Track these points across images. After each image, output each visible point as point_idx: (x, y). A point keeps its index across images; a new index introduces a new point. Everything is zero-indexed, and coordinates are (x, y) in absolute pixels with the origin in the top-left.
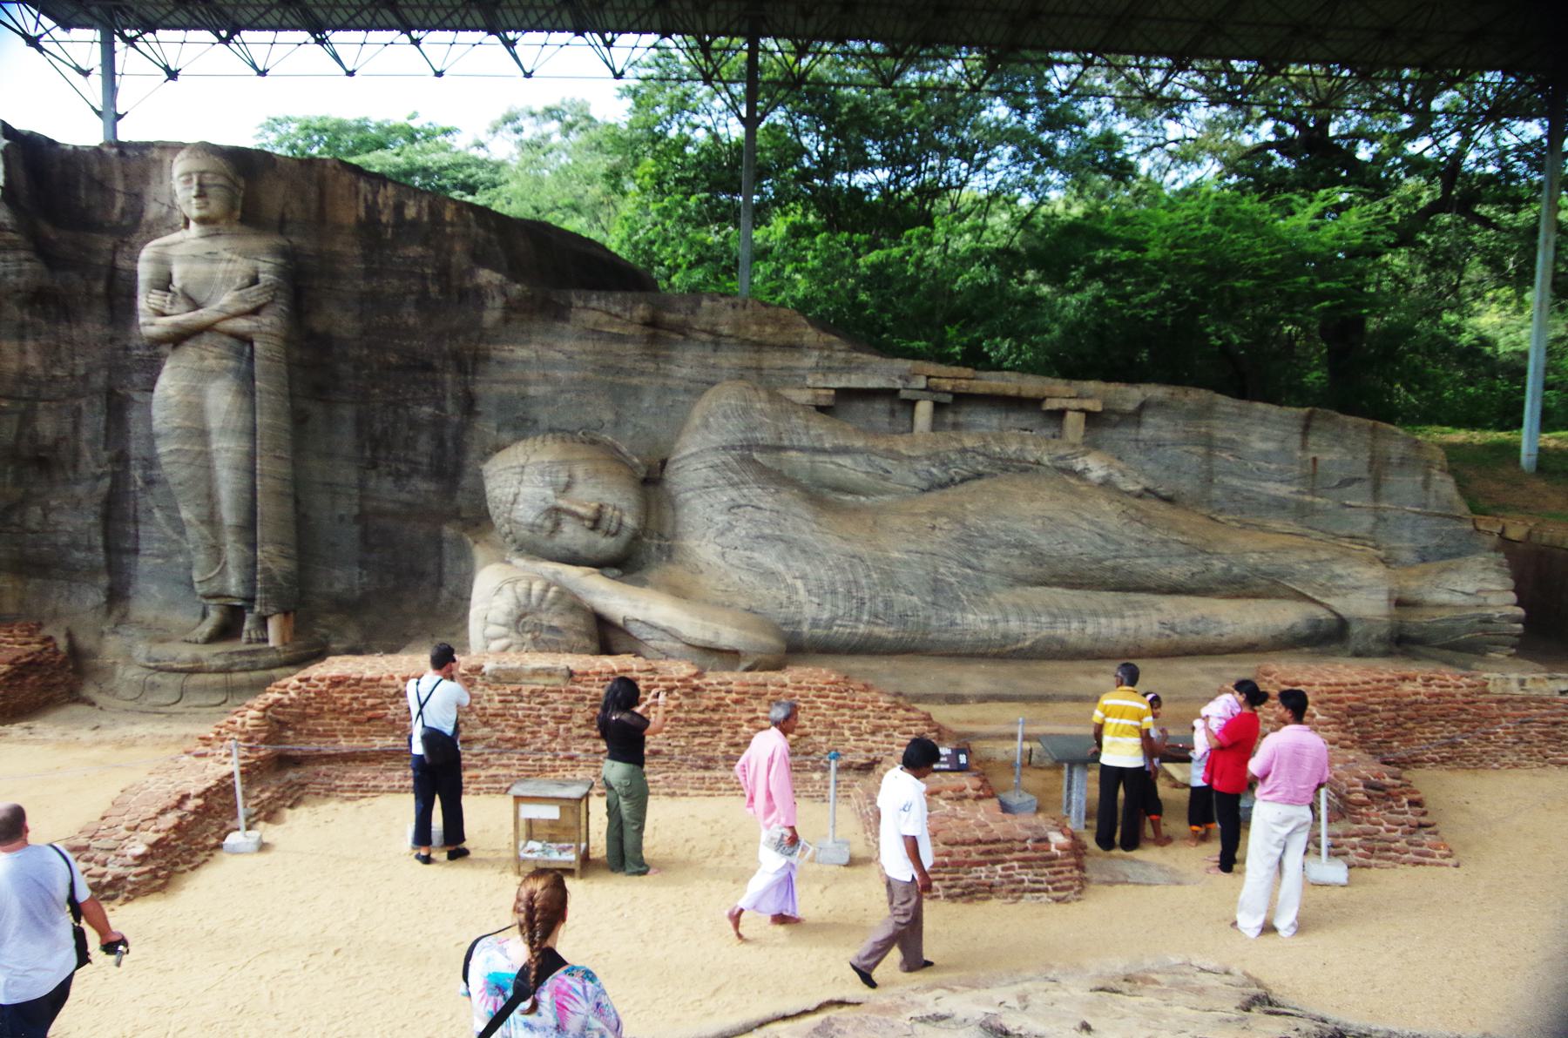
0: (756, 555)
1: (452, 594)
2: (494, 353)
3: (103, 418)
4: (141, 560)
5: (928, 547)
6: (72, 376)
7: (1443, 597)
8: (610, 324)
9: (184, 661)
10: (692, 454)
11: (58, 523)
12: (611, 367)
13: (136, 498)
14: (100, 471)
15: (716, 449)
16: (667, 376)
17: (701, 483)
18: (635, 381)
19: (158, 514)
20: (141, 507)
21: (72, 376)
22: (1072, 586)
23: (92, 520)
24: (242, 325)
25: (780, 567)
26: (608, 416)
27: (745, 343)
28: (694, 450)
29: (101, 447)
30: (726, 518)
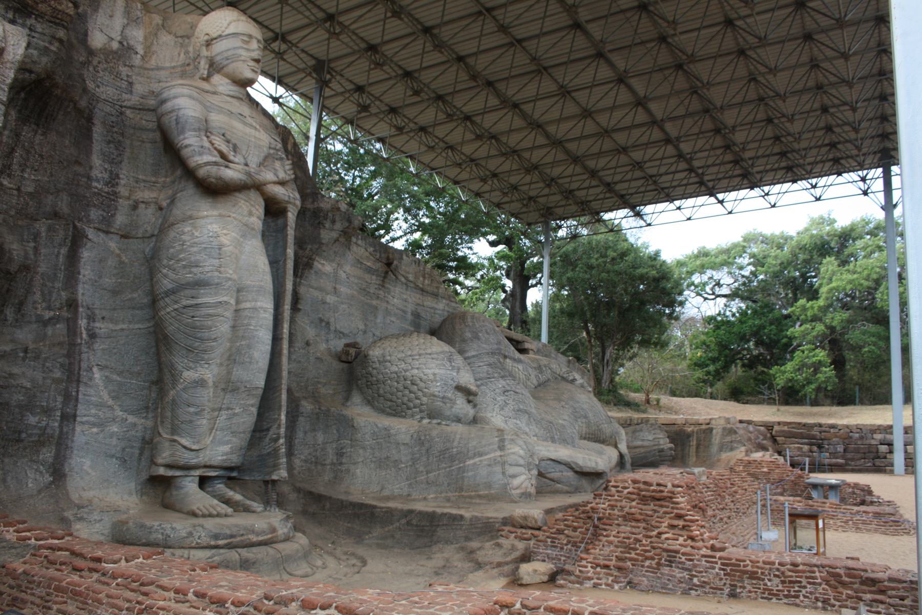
0: (518, 422)
1: (306, 461)
2: (316, 263)
3: (64, 251)
4: (78, 429)
5: (567, 418)
6: (18, 189)
7: (639, 443)
8: (368, 259)
9: (263, 532)
10: (473, 356)
11: (11, 375)
12: (364, 290)
13: (80, 353)
14: (48, 315)
15: (488, 354)
16: (388, 302)
17: (485, 375)
18: (374, 302)
19: (97, 375)
20: (84, 365)
21: (18, 189)
22: (589, 439)
23: (57, 374)
24: (279, 191)
25: (528, 430)
26: (361, 327)
27: (417, 287)
28: (473, 353)
29: (58, 285)
30: (503, 398)
